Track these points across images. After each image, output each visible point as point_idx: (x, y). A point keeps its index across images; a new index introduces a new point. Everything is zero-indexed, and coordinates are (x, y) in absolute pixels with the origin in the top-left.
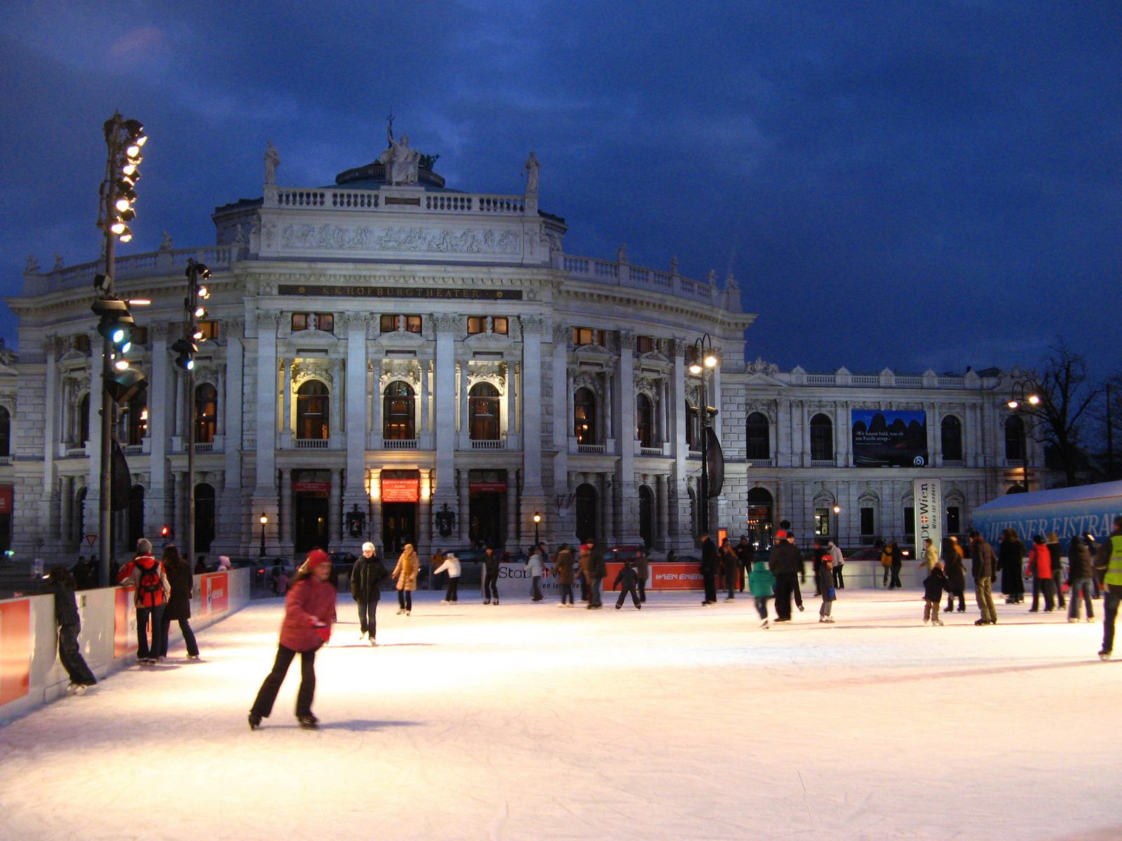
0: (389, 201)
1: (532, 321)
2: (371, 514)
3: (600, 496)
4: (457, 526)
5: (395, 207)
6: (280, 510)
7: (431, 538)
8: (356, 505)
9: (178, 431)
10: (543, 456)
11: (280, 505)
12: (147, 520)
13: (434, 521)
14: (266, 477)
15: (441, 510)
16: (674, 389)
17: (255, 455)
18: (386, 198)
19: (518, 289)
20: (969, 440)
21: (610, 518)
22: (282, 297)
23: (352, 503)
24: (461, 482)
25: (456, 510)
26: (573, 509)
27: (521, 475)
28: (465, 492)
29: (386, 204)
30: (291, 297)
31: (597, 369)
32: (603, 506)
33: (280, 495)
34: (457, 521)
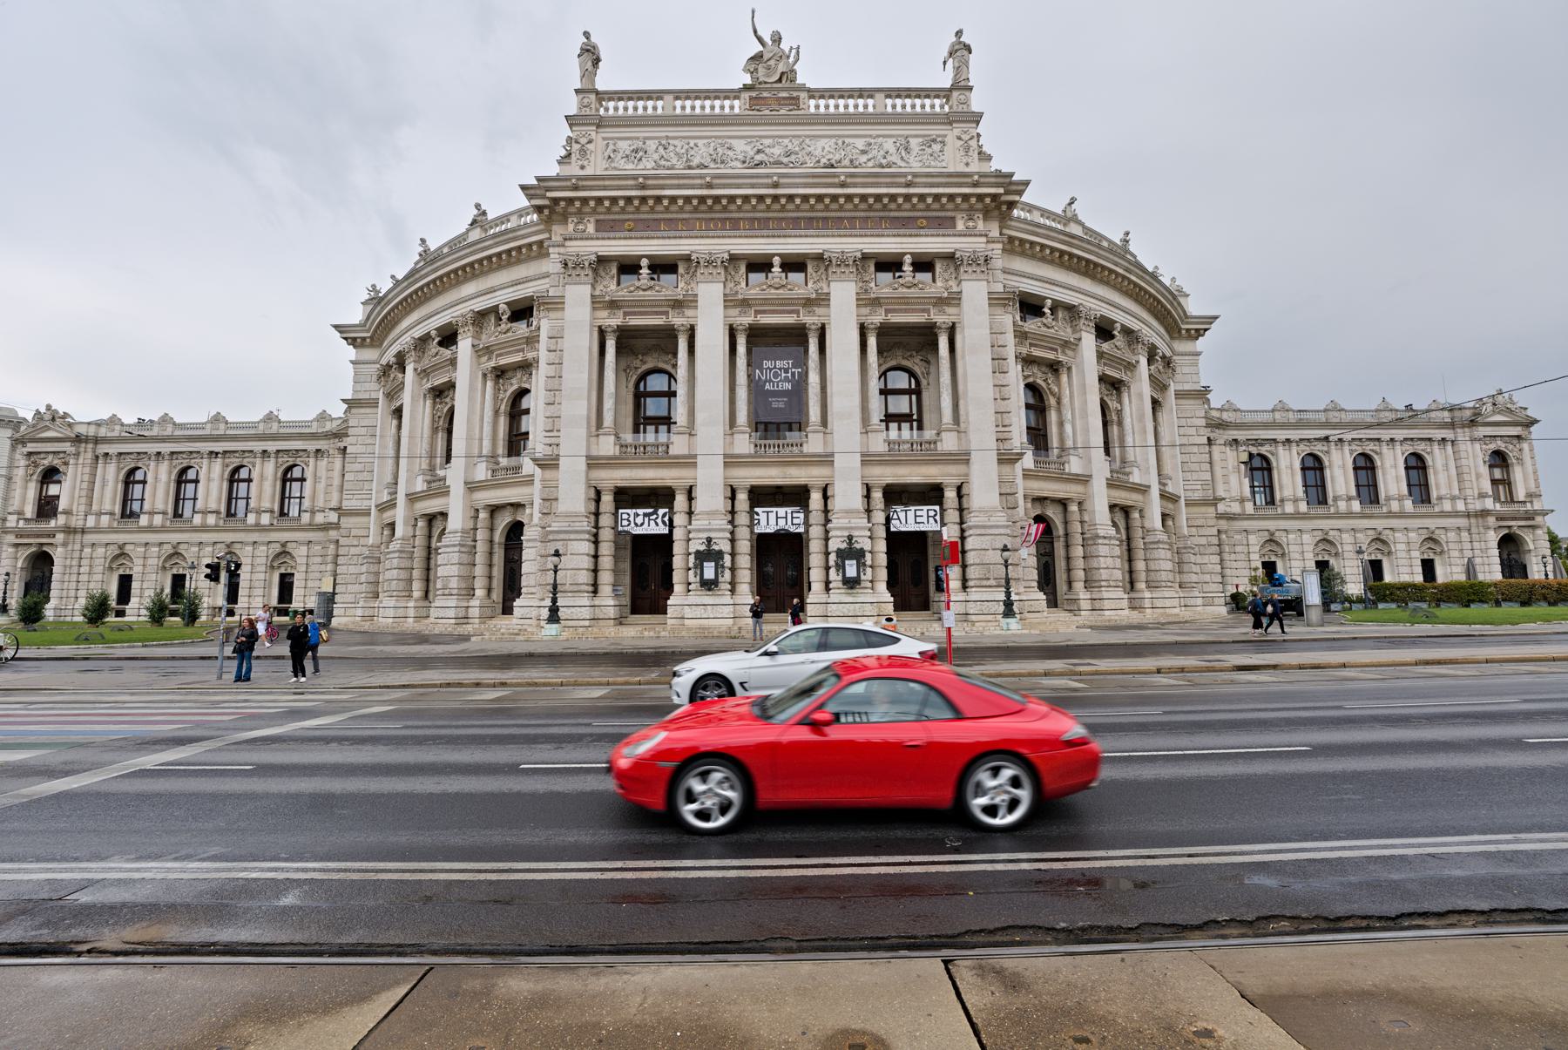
1: (974, 261)
2: (733, 555)
3: (1061, 532)
4: (869, 570)
6: (597, 549)
7: (827, 589)
9: (485, 452)
10: (1000, 461)
11: (596, 542)
12: (441, 571)
13: (832, 563)
14: (573, 499)
15: (844, 546)
16: (1140, 396)
17: (556, 466)
19: (949, 214)
20: (1440, 480)
21: (1079, 563)
22: (600, 235)
23: (705, 535)
24: (873, 503)
25: (866, 544)
26: (1033, 550)
27: (964, 491)
30: (612, 235)
31: (1050, 356)
32: (1067, 546)
33: (597, 527)
34: (869, 562)
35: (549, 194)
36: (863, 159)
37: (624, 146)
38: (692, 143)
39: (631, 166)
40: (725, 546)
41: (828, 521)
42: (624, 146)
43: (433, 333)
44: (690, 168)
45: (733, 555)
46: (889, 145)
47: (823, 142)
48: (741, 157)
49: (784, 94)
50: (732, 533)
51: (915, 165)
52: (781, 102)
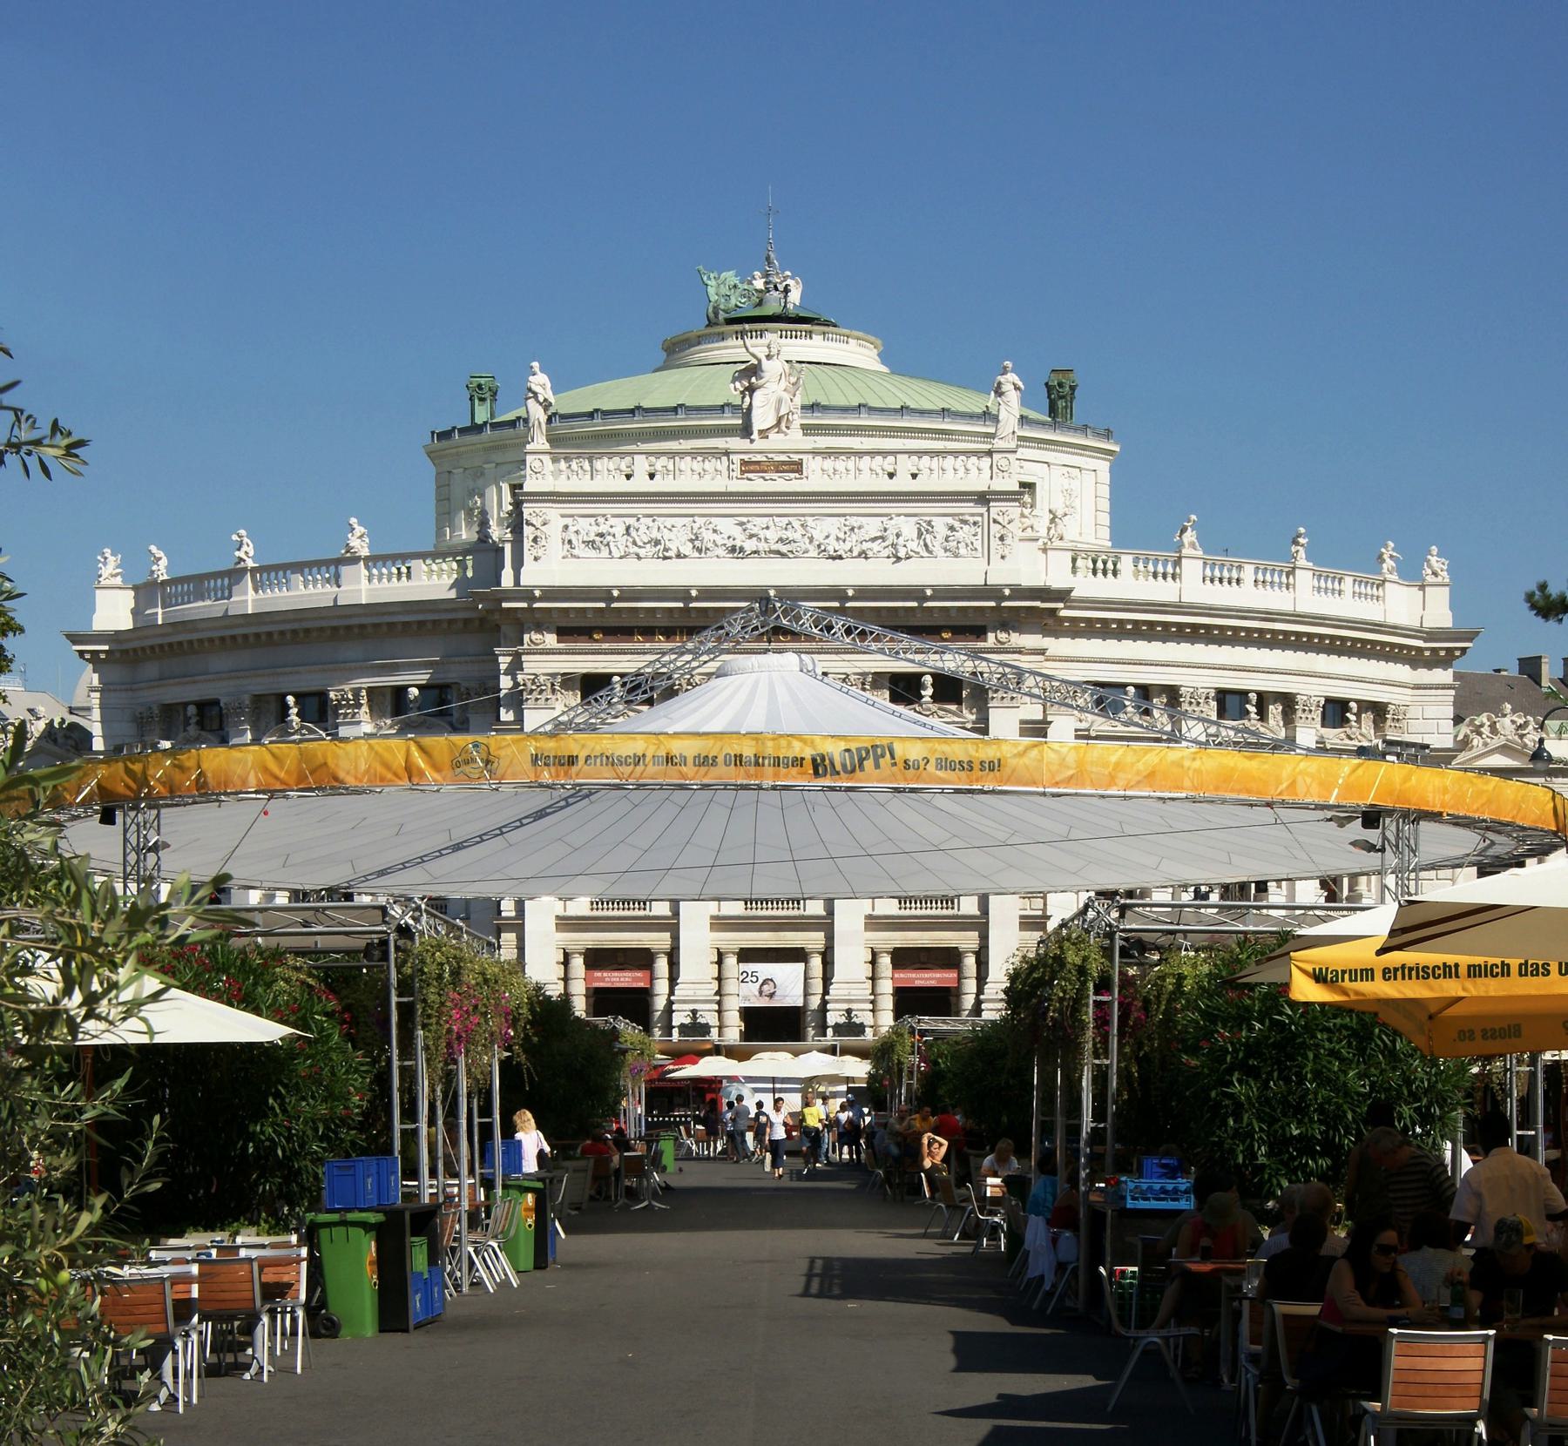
0: (748, 467)
5: (758, 484)
8: (694, 1012)
18: (744, 463)
28: (886, 987)
29: (743, 472)
35: (504, 605)
36: (876, 546)
37: (583, 524)
38: (669, 522)
39: (593, 553)
40: (710, 1018)
41: (826, 992)
42: (587, 528)
43: (290, 699)
44: (665, 558)
45: (720, 1028)
46: (908, 528)
47: (831, 526)
48: (730, 543)
49: (783, 458)
50: (719, 1003)
51: (938, 550)
52: (780, 467)
